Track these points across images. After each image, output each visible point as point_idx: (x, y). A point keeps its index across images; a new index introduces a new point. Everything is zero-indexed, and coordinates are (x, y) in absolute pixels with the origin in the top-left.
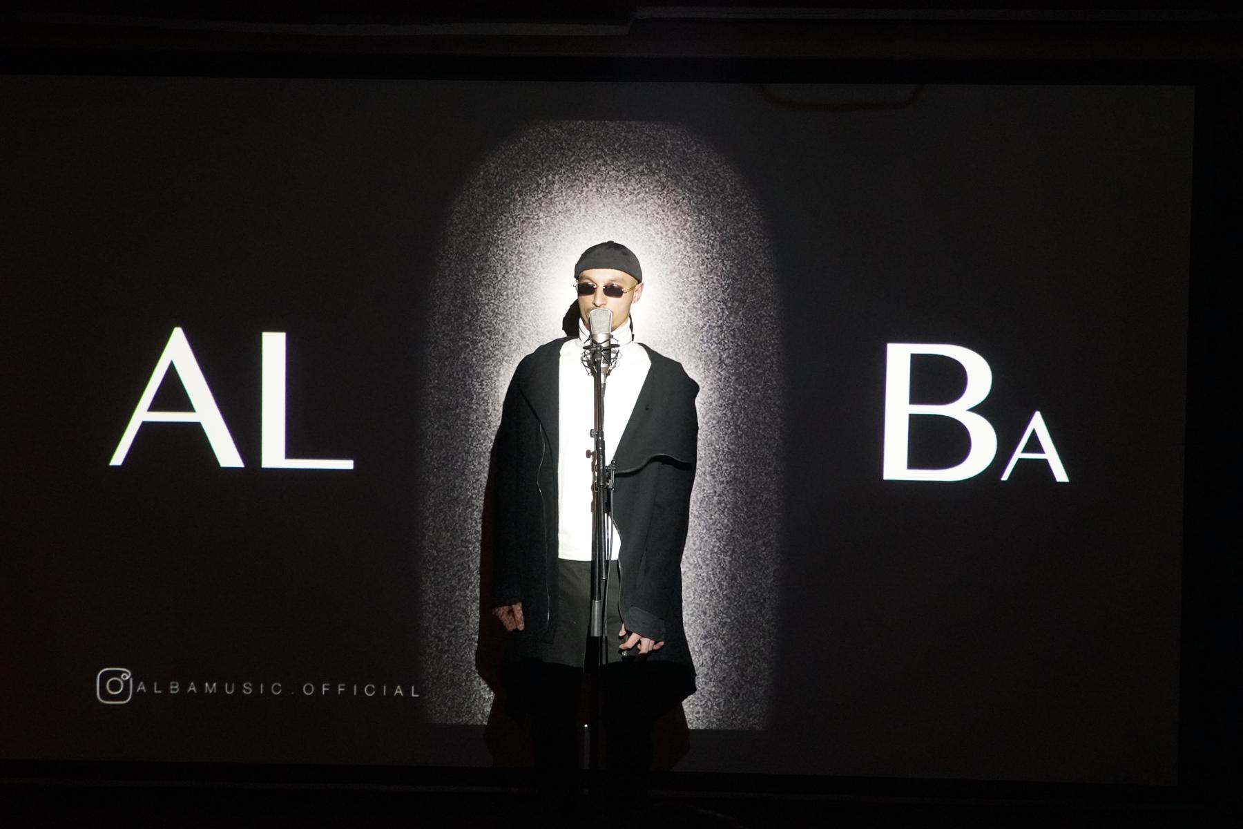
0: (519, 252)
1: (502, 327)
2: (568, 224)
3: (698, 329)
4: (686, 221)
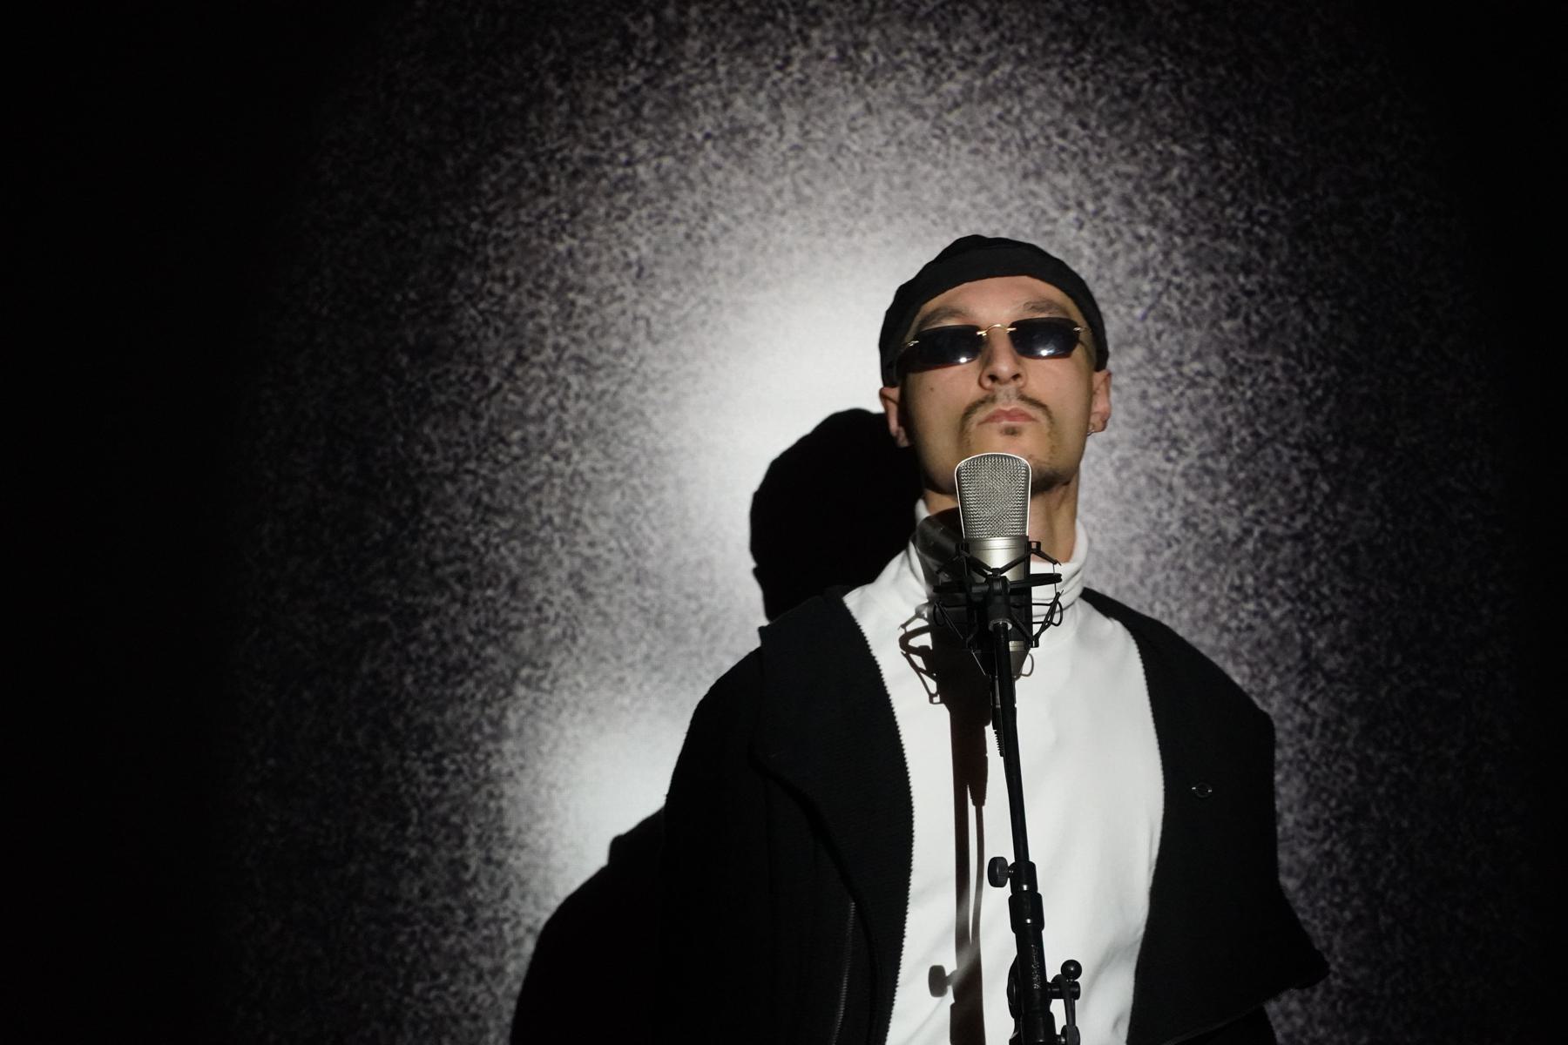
0: (565, 286)
2: (740, 179)
3: (1221, 551)
4: (1168, 160)
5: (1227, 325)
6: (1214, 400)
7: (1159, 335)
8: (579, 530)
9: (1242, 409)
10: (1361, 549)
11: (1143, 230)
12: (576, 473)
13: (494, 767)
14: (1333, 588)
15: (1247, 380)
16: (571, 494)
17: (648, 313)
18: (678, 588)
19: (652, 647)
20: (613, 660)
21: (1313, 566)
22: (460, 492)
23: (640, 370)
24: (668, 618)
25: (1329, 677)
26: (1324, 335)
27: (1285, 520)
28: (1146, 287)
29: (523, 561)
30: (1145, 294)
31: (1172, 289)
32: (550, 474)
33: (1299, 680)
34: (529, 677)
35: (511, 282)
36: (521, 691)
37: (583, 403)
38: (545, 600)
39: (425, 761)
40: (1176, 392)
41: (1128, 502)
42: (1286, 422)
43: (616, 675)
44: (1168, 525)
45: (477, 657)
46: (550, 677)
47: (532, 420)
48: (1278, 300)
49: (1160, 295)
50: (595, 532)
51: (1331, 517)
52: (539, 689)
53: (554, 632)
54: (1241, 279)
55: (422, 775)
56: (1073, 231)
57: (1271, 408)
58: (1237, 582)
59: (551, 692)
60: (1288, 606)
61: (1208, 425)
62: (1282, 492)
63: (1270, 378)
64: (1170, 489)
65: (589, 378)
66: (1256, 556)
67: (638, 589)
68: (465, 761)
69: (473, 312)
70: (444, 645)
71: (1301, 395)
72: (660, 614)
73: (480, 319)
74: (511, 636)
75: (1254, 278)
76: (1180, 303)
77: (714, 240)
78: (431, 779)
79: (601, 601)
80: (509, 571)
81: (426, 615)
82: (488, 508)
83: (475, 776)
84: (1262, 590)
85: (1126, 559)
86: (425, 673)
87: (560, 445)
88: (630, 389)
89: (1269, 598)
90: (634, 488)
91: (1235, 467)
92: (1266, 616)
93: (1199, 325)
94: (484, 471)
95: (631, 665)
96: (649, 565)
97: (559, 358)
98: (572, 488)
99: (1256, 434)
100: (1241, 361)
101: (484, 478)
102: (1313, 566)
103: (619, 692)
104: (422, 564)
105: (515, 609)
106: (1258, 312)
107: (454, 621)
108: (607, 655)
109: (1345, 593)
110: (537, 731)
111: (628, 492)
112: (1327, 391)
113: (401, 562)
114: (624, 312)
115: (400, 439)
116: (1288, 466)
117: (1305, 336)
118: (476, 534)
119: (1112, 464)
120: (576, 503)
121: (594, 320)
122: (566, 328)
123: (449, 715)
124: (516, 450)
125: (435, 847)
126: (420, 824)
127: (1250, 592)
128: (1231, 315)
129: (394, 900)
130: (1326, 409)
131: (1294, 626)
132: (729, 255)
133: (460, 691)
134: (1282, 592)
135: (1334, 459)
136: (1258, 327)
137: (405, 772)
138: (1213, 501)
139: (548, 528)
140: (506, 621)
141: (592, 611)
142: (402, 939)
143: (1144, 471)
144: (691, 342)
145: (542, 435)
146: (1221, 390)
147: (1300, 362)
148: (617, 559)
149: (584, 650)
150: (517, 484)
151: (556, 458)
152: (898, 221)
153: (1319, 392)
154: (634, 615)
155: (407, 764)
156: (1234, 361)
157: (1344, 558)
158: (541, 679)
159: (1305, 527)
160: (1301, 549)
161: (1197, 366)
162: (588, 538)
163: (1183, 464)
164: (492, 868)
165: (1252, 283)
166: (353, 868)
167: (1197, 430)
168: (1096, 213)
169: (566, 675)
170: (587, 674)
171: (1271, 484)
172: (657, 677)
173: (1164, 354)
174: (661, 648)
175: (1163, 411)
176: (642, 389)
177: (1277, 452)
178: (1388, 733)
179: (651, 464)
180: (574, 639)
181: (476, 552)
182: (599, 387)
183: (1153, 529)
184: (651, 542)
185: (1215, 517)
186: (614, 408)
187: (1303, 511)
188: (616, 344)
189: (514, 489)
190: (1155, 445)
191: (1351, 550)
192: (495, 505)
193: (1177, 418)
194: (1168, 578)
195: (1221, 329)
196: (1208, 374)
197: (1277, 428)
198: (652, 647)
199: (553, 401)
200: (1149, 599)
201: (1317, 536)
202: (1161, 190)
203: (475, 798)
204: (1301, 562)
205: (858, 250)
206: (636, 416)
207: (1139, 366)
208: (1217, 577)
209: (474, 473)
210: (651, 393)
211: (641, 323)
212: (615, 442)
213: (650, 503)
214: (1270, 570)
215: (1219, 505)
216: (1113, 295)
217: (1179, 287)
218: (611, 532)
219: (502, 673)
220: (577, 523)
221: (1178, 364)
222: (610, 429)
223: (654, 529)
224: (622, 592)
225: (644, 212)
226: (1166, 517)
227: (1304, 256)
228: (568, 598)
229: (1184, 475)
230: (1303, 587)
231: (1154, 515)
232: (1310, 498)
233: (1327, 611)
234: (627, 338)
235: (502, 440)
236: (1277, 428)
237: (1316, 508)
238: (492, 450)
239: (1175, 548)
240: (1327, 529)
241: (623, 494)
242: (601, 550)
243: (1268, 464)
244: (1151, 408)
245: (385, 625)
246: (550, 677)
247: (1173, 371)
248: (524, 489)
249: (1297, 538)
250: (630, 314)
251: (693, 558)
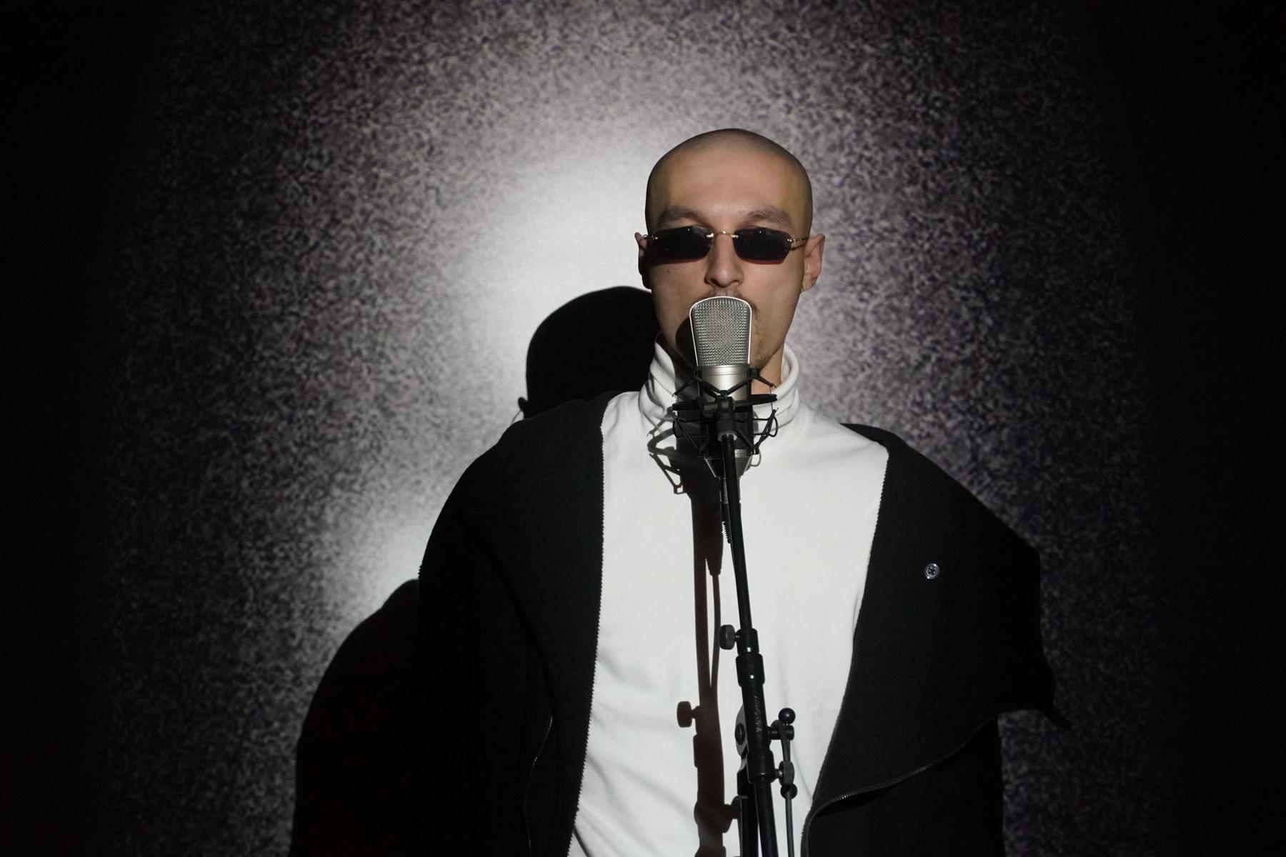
0: (370, 162)
1: (327, 383)
3: (903, 374)
5: (908, 190)
6: (898, 251)
7: (853, 199)
8: (383, 361)
9: (921, 258)
10: (1019, 371)
11: (840, 114)
12: (380, 314)
13: (315, 554)
14: (996, 403)
15: (925, 235)
16: (376, 332)
17: (438, 184)
18: (464, 408)
19: (442, 455)
20: (412, 468)
22: (286, 330)
23: (431, 231)
24: (456, 433)
25: (993, 475)
26: (987, 198)
27: (956, 348)
28: (843, 160)
29: (338, 386)
30: (842, 166)
31: (864, 161)
32: (359, 315)
33: (969, 478)
34: (343, 481)
35: (326, 160)
36: (336, 492)
37: (385, 258)
38: (355, 418)
39: (259, 549)
40: (867, 245)
41: (830, 335)
42: (957, 268)
43: (413, 479)
44: (863, 352)
45: (301, 464)
46: (360, 480)
47: (345, 271)
48: (950, 169)
49: (854, 166)
50: (395, 362)
51: (994, 345)
52: (350, 490)
53: (363, 444)
54: (920, 153)
55: (257, 561)
56: (783, 115)
57: (945, 257)
58: (918, 399)
59: (361, 493)
60: (960, 418)
61: (894, 271)
62: (954, 326)
63: (943, 233)
64: (863, 324)
65: (390, 237)
66: (933, 378)
67: (431, 409)
68: (291, 549)
69: (295, 183)
70: (274, 456)
71: (969, 246)
72: (450, 429)
73: (301, 190)
74: (328, 447)
75: (930, 152)
76: (870, 173)
77: (491, 124)
78: (263, 564)
79: (401, 418)
80: (326, 395)
81: (258, 431)
82: (309, 343)
83: (300, 561)
84: (938, 405)
85: (828, 381)
86: (257, 478)
87: (367, 292)
88: (423, 246)
89: (945, 412)
90: (427, 326)
91: (916, 306)
92: (942, 426)
93: (886, 191)
94: (305, 314)
95: (426, 471)
96: (439, 389)
97: (366, 221)
98: (377, 327)
99: (932, 279)
100: (920, 220)
101: (305, 318)
102: (981, 384)
103: (416, 492)
104: (255, 389)
105: (331, 426)
106: (933, 180)
107: (281, 435)
108: (406, 462)
110: (350, 525)
111: (422, 329)
112: (991, 243)
113: (238, 388)
114: (418, 183)
115: (237, 287)
116: (959, 304)
117: (972, 199)
118: (299, 364)
119: (816, 304)
120: (380, 339)
121: (393, 190)
122: (371, 196)
123: (278, 512)
124: (331, 296)
125: (267, 619)
126: (256, 600)
127: (929, 406)
128: (912, 182)
129: (234, 663)
130: (989, 258)
131: (965, 433)
132: (504, 136)
133: (286, 493)
134: (955, 407)
135: (996, 299)
136: (933, 192)
137: (242, 559)
138: (898, 334)
139: (357, 359)
140: (323, 436)
141: (394, 427)
142: (242, 694)
143: (842, 310)
144: (473, 208)
145: (352, 283)
146: (904, 242)
148: (414, 384)
149: (388, 458)
150: (332, 323)
151: (363, 302)
152: (641, 108)
153: (984, 244)
154: (428, 430)
155: (244, 552)
156: (915, 219)
157: (1005, 378)
158: (353, 482)
159: (973, 353)
160: (970, 371)
161: (884, 224)
162: (390, 367)
163: (874, 302)
164: (313, 636)
165: (929, 156)
166: (201, 637)
167: (884, 276)
168: (801, 100)
169: (374, 479)
170: (390, 478)
171: (945, 319)
173: (858, 214)
174: (450, 456)
175: (857, 260)
176: (433, 246)
177: (950, 293)
178: (1041, 520)
179: (440, 306)
180: (379, 449)
181: (299, 378)
182: (398, 244)
183: (850, 357)
184: (441, 370)
185: (900, 346)
186: (410, 261)
187: (972, 341)
188: (412, 209)
189: (330, 328)
190: (851, 288)
191: (1011, 372)
192: (315, 340)
193: (868, 266)
194: (862, 395)
195: (904, 194)
196: (893, 230)
197: (950, 274)
198: (442, 455)
199: (360, 256)
200: (847, 413)
201: (983, 361)
202: (854, 81)
203: (300, 580)
204: (970, 383)
205: (608, 132)
206: (429, 268)
207: (837, 223)
208: (901, 394)
209: (297, 315)
210: (441, 249)
211: (432, 192)
212: (411, 289)
213: (440, 339)
214: (945, 389)
215: (903, 336)
216: (816, 166)
217: (869, 160)
218: (409, 362)
219: (321, 477)
220: (381, 355)
221: (869, 222)
222: (408, 279)
223: (444, 360)
224: (418, 411)
225: (434, 102)
226: (860, 347)
227: (970, 134)
228: (375, 416)
229: (874, 312)
230: (972, 403)
231: (850, 345)
232: (977, 331)
233: (991, 423)
234: (421, 204)
235: (320, 288)
236: (950, 274)
237: (982, 339)
238: (311, 296)
239: (868, 371)
240: (991, 355)
241: (418, 332)
242: (400, 377)
243: (942, 303)
244: (847, 258)
245: (225, 439)
246: (360, 480)
247: (865, 228)
248: (337, 328)
249: (965, 362)
250: (422, 185)
251: (476, 383)
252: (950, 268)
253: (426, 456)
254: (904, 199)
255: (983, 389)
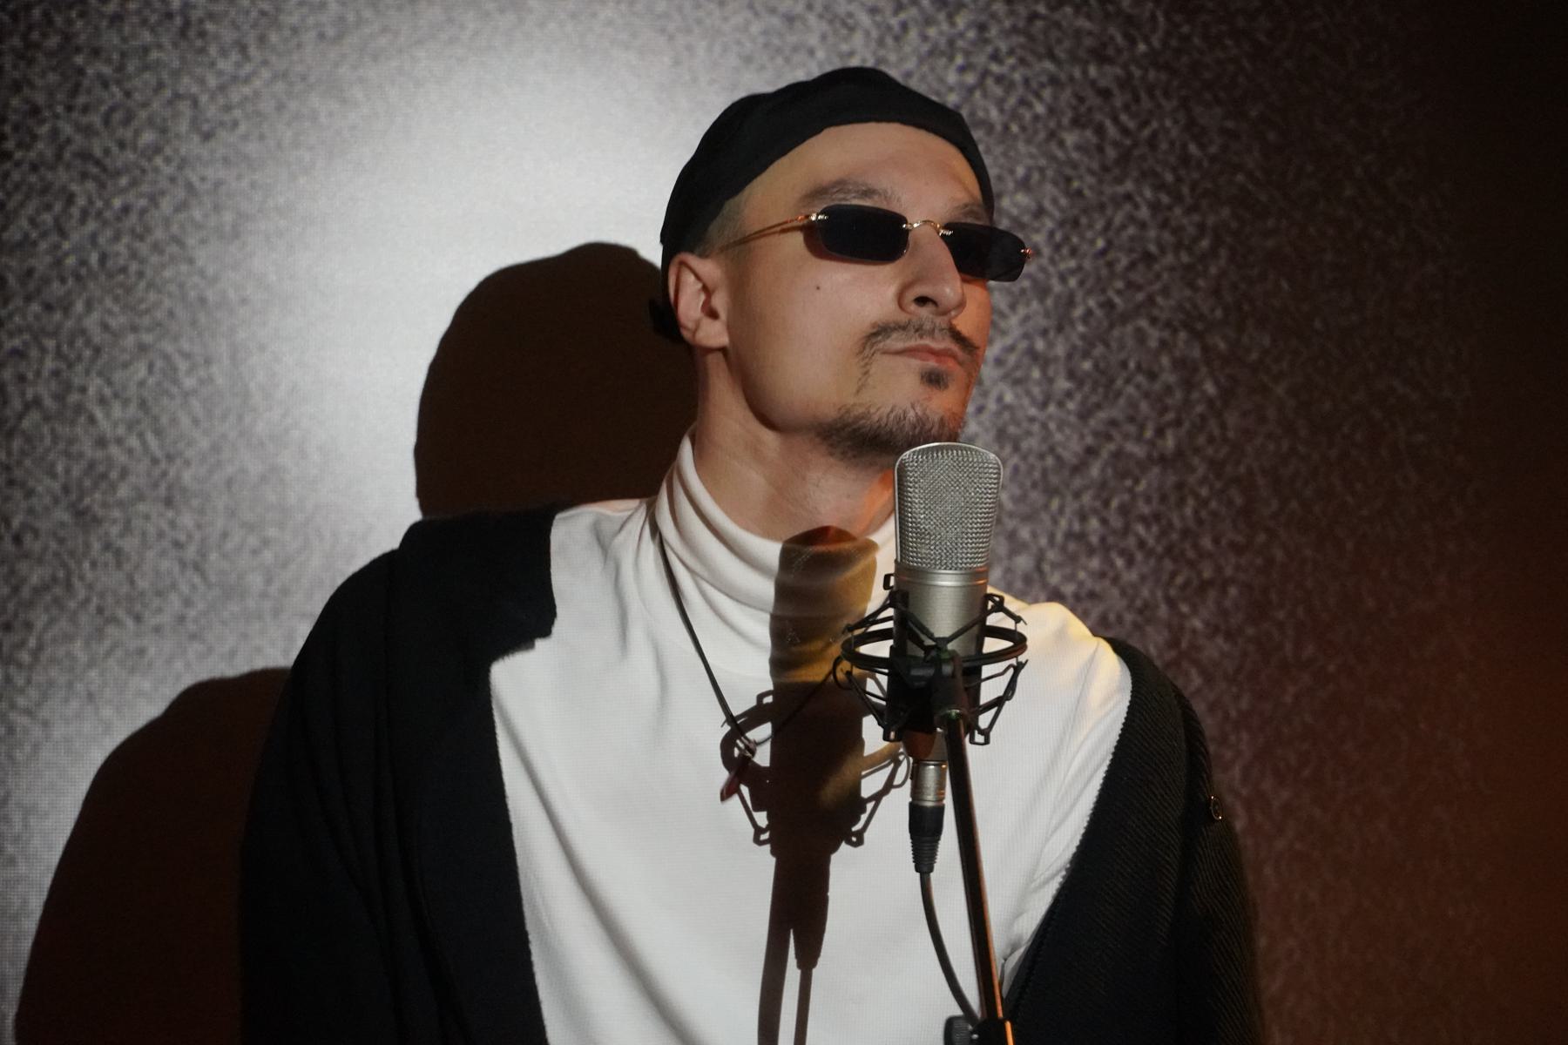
5: (1071, 138)
6: (1046, 251)
14: (1216, 541)
18: (232, 513)
19: (187, 602)
20: (130, 623)
21: (1188, 511)
24: (213, 556)
26: (1213, 159)
42: (1157, 286)
43: (133, 645)
51: (1217, 432)
57: (1132, 266)
58: (1077, 527)
62: (1147, 395)
65: (102, 186)
67: (170, 514)
71: (1178, 247)
76: (1000, 104)
79: (114, 530)
84: (1111, 540)
89: (1123, 553)
90: (166, 357)
92: (1116, 580)
95: (157, 630)
99: (1108, 305)
103: (132, 671)
108: (121, 613)
109: (1237, 549)
111: (159, 364)
116: (1157, 354)
117: (1185, 159)
127: (1094, 540)
128: (1076, 123)
131: (1159, 594)
134: (1142, 544)
136: (1116, 144)
141: (96, 546)
144: (262, 137)
147: (1178, 198)
153: (1205, 243)
154: (163, 554)
156: (1079, 193)
160: (1172, 479)
171: (1128, 381)
172: (197, 647)
174: (201, 606)
176: (182, 207)
179: (194, 323)
187: (1178, 423)
188: (148, 137)
195: (1061, 144)
197: (1140, 297)
198: (187, 602)
204: (1173, 499)
208: (1045, 517)
214: (1124, 510)
215: (1052, 409)
218: (131, 425)
222: (134, 267)
223: (196, 422)
224: (147, 517)
230: (1175, 536)
233: (1207, 574)
240: (1210, 451)
241: (151, 367)
252: (1139, 288)
253: (156, 602)
254: (1060, 154)
255: (1196, 512)
